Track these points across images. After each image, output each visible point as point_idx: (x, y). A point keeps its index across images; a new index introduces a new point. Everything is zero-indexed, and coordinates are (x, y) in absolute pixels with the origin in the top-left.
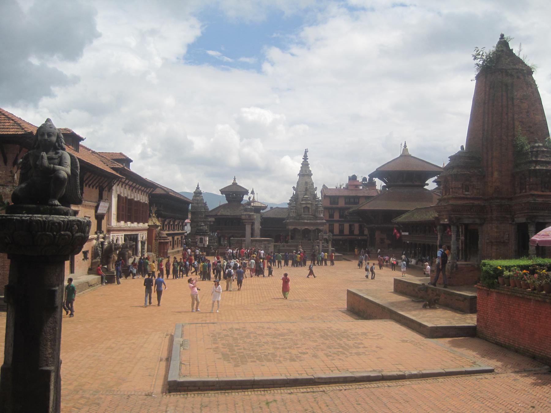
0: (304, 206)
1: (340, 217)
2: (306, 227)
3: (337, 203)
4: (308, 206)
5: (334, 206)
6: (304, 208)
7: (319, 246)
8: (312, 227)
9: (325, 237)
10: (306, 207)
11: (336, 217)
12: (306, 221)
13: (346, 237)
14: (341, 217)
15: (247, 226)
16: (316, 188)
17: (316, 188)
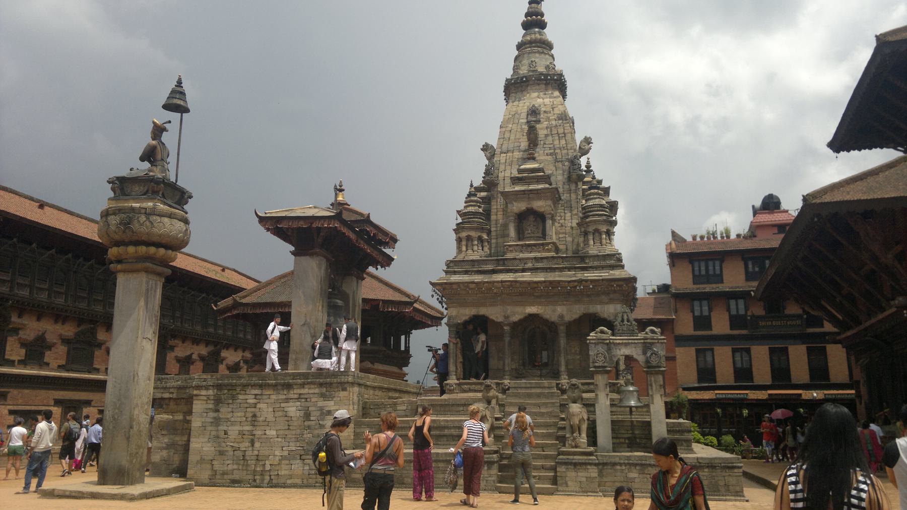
0: (520, 206)
1: (731, 329)
2: (532, 310)
3: (719, 279)
4: (539, 205)
5: (708, 288)
6: (521, 217)
7: (590, 406)
8: (560, 309)
9: (626, 351)
10: (530, 212)
11: (720, 325)
12: (527, 277)
13: (762, 395)
14: (736, 321)
15: (121, 279)
16: (588, 141)
17: (588, 141)
